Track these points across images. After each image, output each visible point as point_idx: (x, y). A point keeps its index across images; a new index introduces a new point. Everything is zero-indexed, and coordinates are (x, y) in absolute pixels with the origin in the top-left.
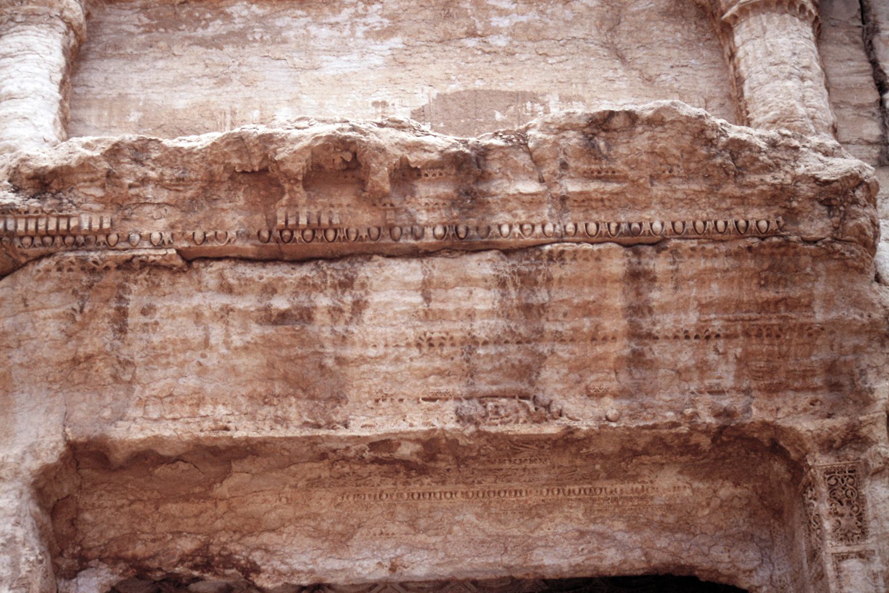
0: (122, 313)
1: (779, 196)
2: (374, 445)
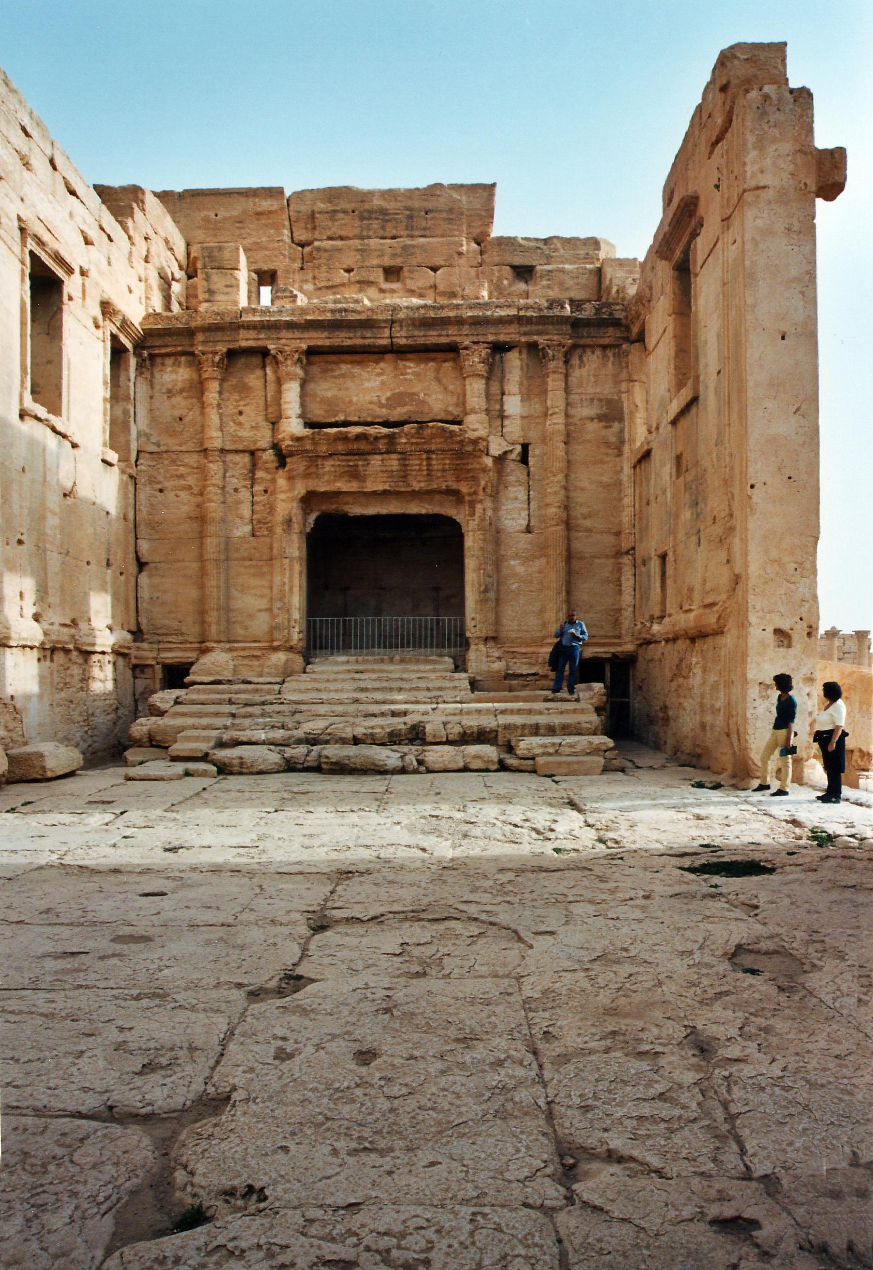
1: (461, 442)
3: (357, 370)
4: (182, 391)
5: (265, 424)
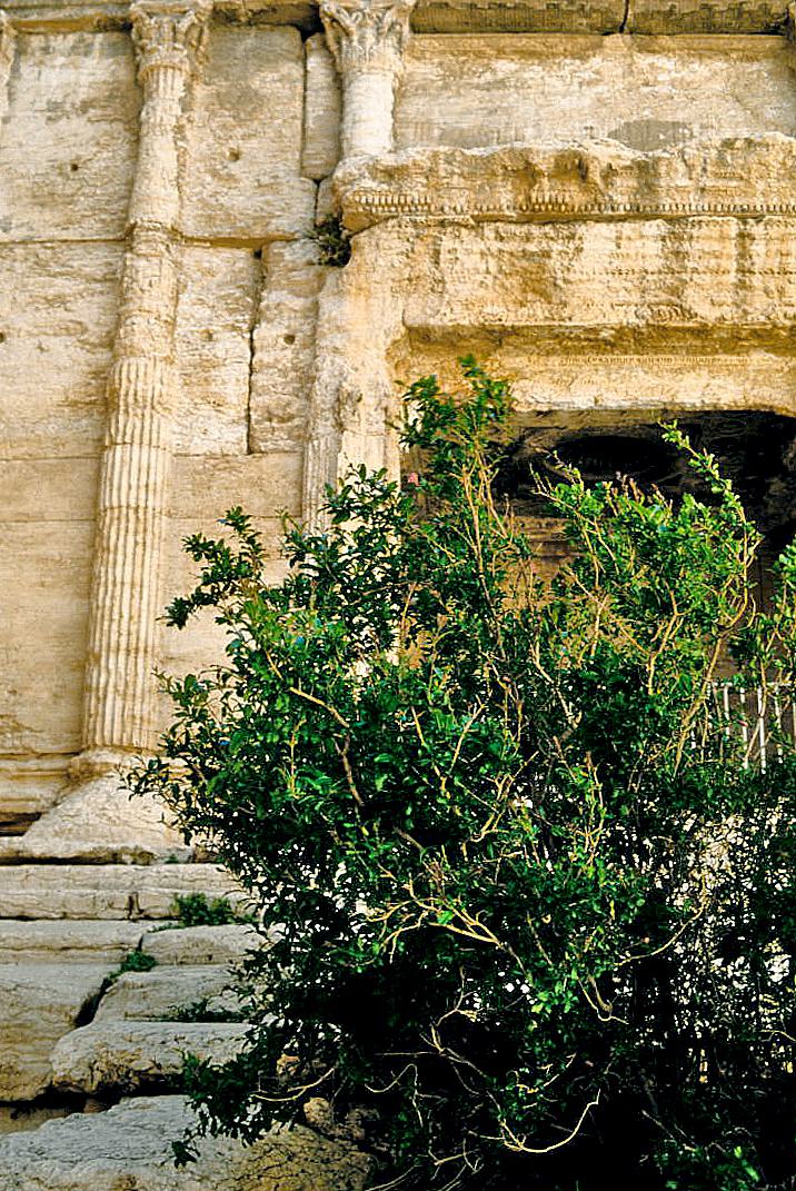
0: (437, 252)
2: (587, 330)
3: (534, 72)
4: (85, 106)
5: (295, 181)
